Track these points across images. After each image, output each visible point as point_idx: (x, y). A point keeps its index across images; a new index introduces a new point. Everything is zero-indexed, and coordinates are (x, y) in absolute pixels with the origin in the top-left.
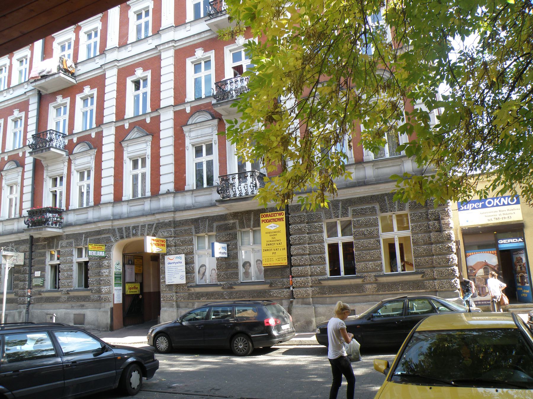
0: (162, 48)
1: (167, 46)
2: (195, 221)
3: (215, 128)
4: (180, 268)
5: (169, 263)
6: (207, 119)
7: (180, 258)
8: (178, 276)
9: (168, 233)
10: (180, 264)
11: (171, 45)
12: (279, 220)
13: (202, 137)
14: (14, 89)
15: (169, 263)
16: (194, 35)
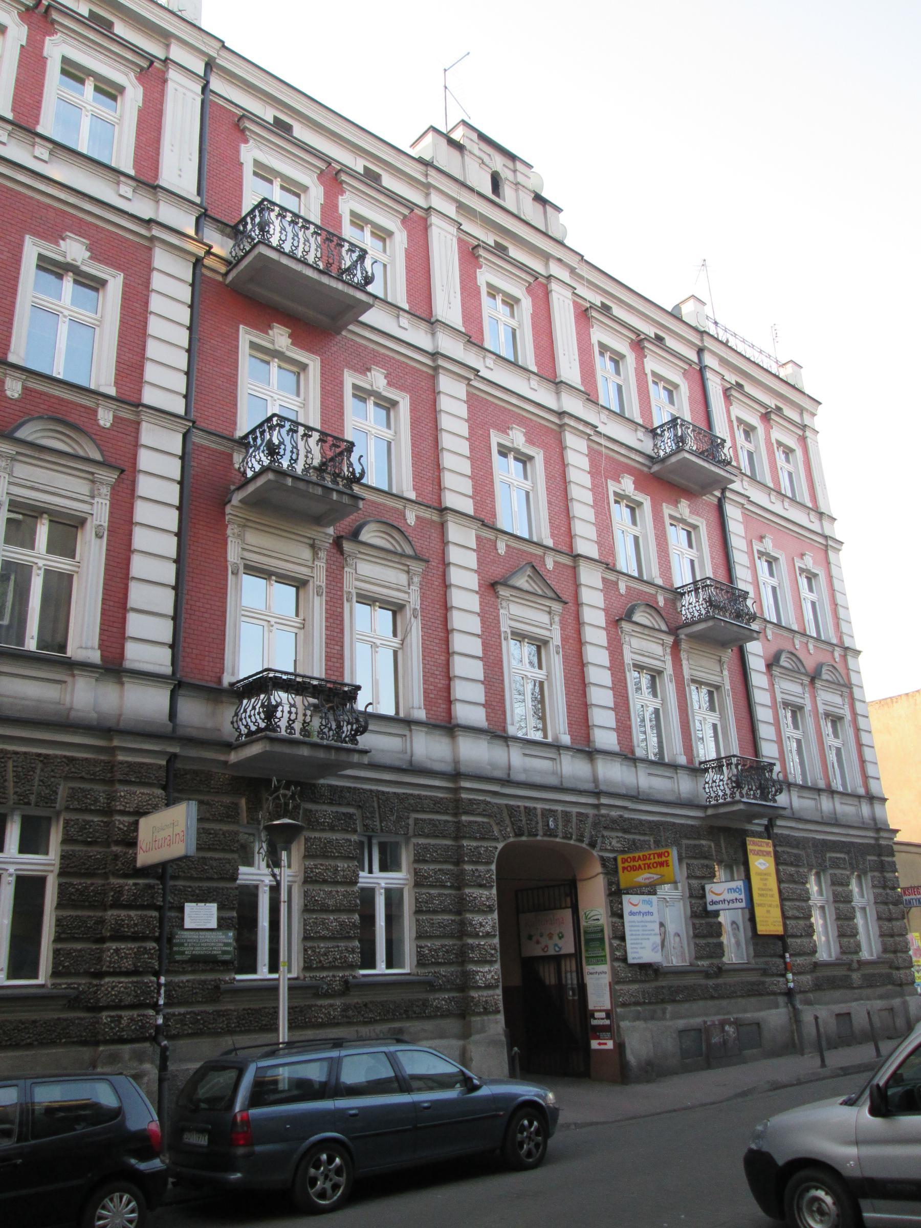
0: (572, 423)
1: (581, 427)
2: (654, 828)
3: (669, 650)
4: (650, 926)
5: (632, 913)
6: (650, 625)
7: (650, 903)
8: (648, 944)
9: (618, 842)
10: (648, 918)
11: (589, 431)
12: (768, 853)
13: (648, 657)
14: (59, 152)
15: (632, 913)
16: (622, 444)
